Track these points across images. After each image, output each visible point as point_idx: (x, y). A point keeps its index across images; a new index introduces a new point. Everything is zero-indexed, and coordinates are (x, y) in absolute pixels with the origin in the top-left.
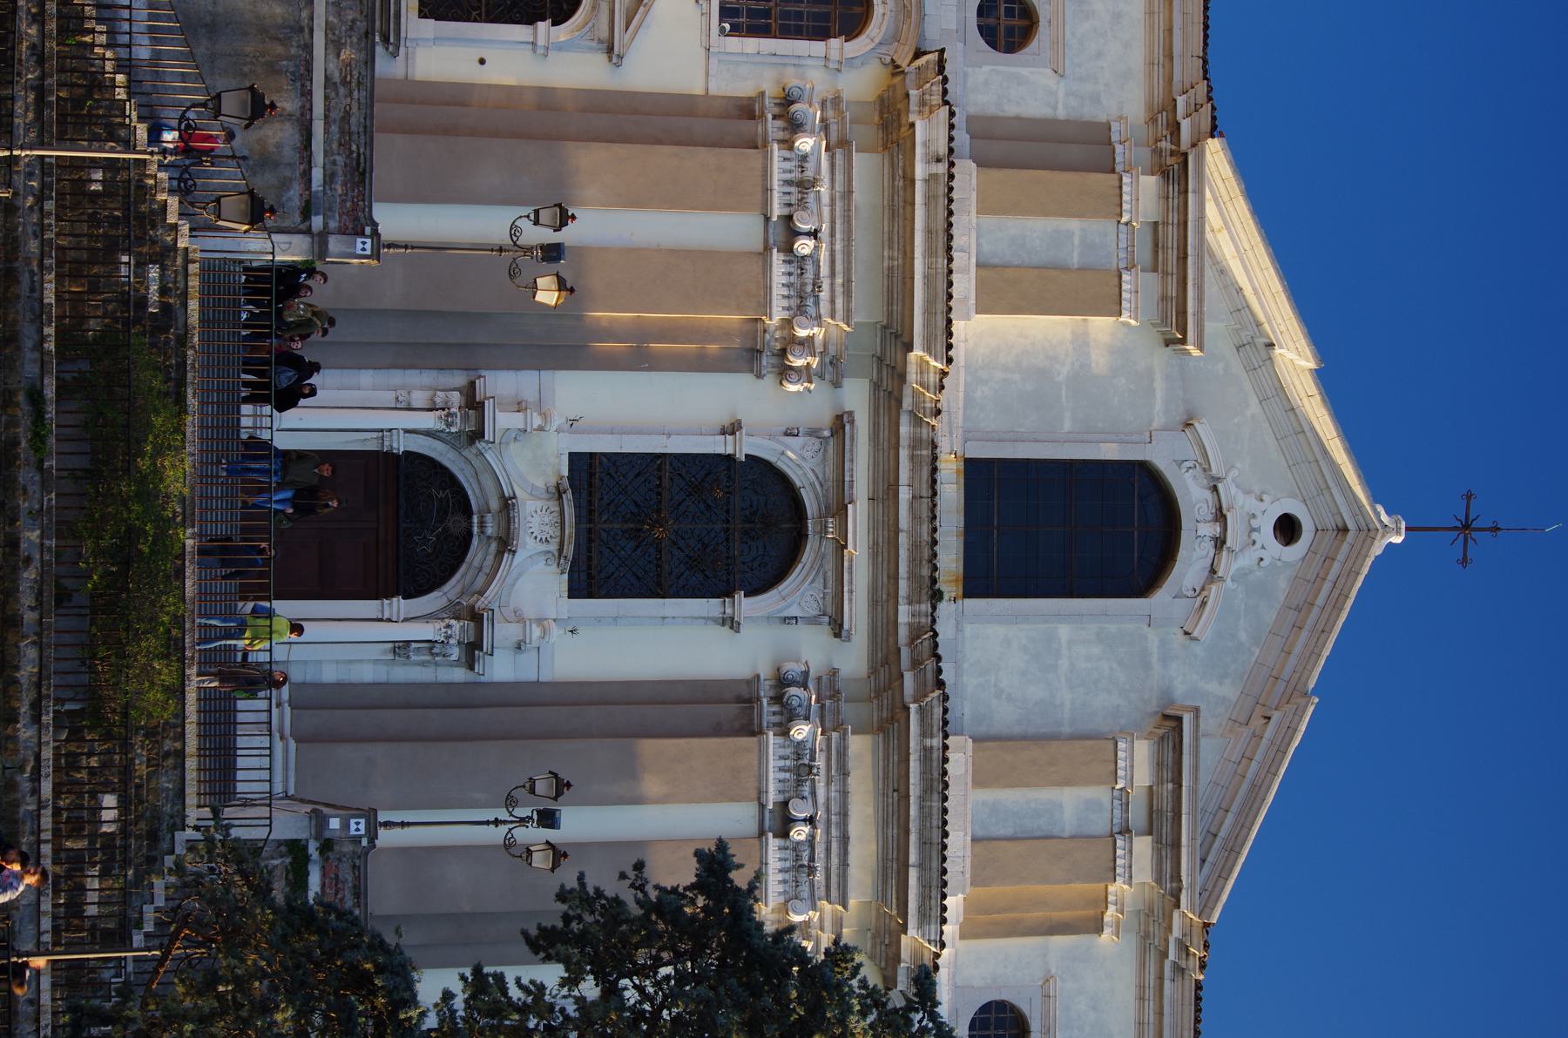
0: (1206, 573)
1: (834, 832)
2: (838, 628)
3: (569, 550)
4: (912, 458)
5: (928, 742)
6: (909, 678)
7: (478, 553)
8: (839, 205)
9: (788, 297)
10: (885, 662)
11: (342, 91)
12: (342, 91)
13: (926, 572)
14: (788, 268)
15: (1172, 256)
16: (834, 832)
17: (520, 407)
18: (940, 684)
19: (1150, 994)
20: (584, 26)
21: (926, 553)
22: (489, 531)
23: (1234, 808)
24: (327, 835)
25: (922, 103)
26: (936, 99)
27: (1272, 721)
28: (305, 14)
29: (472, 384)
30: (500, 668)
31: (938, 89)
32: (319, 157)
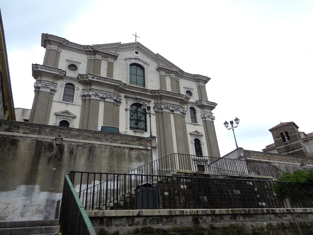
2: (150, 102)
4: (131, 89)
6: (156, 94)
8: (99, 91)
9: (111, 100)
10: (154, 97)
14: (107, 99)
15: (106, 55)
18: (158, 90)
19: (185, 78)
21: (142, 89)
28: (108, 147)
32: (137, 147)
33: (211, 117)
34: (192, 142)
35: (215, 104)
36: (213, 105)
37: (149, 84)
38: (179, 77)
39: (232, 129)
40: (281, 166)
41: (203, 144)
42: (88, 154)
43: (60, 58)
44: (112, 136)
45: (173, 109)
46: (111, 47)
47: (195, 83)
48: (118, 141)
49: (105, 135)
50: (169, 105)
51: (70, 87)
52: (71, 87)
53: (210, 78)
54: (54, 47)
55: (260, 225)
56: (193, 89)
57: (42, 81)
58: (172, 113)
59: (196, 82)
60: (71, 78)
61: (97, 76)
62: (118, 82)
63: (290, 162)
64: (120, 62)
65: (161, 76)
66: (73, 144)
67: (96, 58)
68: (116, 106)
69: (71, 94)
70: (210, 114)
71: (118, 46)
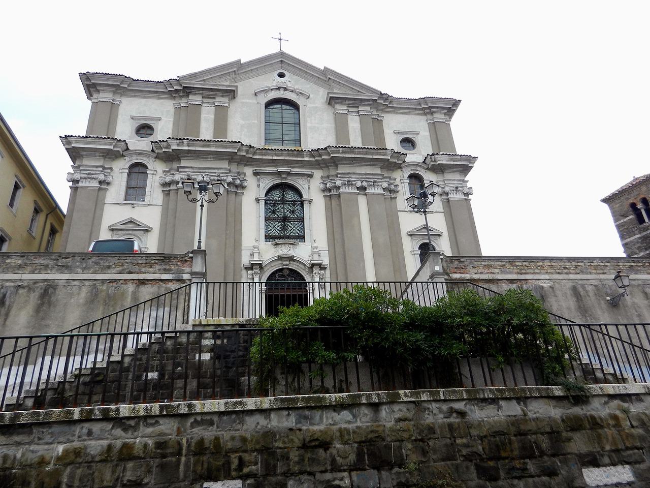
1: (364, 176)
2: (311, 176)
4: (265, 155)
6: (323, 157)
7: (293, 266)
8: (195, 170)
10: (319, 165)
13: (296, 153)
15: (211, 93)
16: (364, 176)
17: (252, 255)
18: (326, 148)
19: (396, 110)
20: (140, 239)
21: (291, 152)
22: (288, 263)
24: (441, 271)
25: (166, 148)
26: (165, 144)
27: (330, 77)
28: (87, 283)
29: (246, 268)
32: (157, 276)
34: (413, 253)
35: (472, 159)
36: (466, 160)
37: (309, 139)
38: (383, 111)
40: (557, 286)
42: (39, 302)
43: (119, 117)
44: (100, 259)
45: (364, 184)
46: (220, 74)
47: (424, 118)
48: (112, 269)
49: (83, 259)
50: (354, 176)
51: (137, 169)
52: (142, 170)
53: (460, 101)
54: (106, 96)
55: (39, 454)
56: (417, 133)
57: (81, 168)
59: (425, 114)
60: (140, 153)
61: (188, 139)
62: (233, 144)
63: (591, 273)
64: (244, 102)
65: (335, 114)
66: (8, 284)
67: (189, 103)
68: (234, 195)
69: (141, 184)
70: (461, 184)
71: (237, 69)
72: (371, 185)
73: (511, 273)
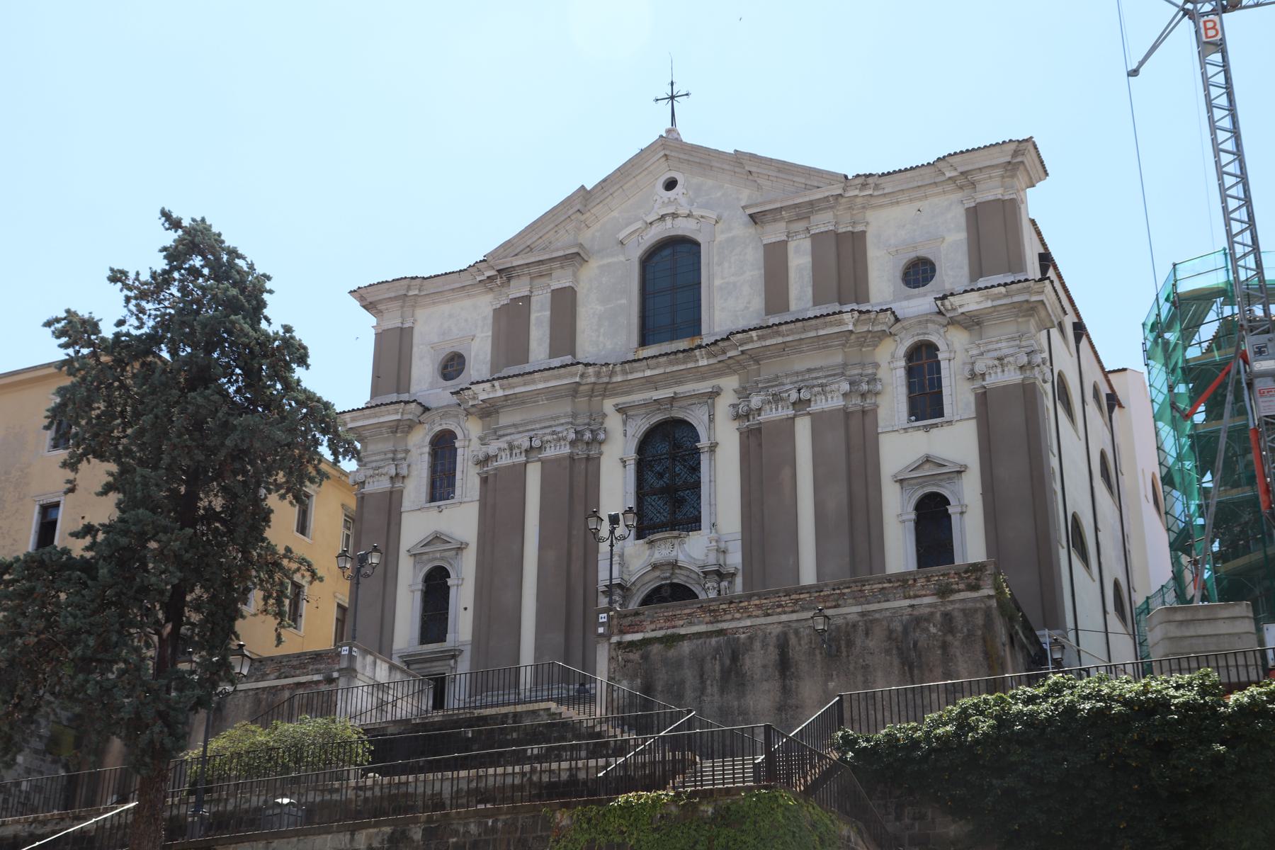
0: (689, 219)
2: (715, 393)
3: (676, 533)
5: (755, 338)
6: (730, 354)
10: (729, 367)
11: (282, 671)
12: (282, 671)
13: (681, 355)
14: (548, 449)
15: (543, 267)
18: (728, 339)
21: (672, 357)
23: (791, 178)
25: (474, 398)
26: (470, 392)
28: (250, 693)
30: (735, 559)
31: (466, 392)
33: (1011, 359)
37: (717, 313)
39: (609, 542)
41: (962, 513)
47: (959, 195)
58: (804, 415)
59: (961, 188)
60: (445, 412)
72: (819, 393)
73: (700, 623)
